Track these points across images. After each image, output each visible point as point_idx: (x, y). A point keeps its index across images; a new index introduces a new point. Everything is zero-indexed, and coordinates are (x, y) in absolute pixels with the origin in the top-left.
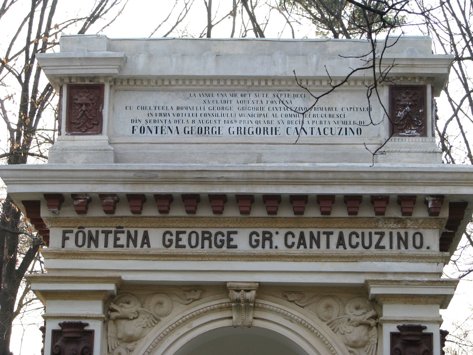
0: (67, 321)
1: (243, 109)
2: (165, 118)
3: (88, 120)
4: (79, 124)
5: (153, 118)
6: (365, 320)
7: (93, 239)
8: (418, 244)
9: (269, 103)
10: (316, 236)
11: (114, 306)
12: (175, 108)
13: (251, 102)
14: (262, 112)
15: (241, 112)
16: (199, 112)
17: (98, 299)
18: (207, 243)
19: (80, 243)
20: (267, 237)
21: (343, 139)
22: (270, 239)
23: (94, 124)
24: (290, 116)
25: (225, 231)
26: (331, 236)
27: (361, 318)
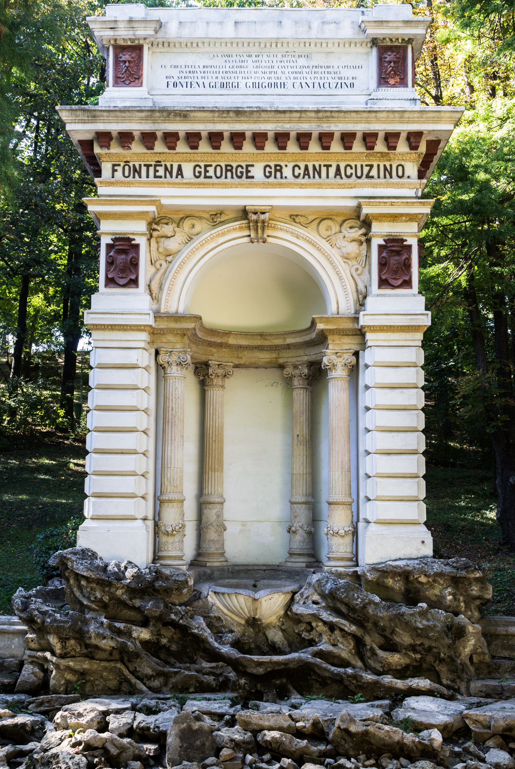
0: (118, 236)
1: (257, 67)
2: (194, 75)
3: (131, 75)
4: (123, 78)
5: (183, 75)
6: (357, 236)
8: (400, 174)
9: (278, 62)
11: (155, 226)
12: (201, 67)
13: (263, 62)
14: (272, 70)
15: (256, 70)
18: (229, 174)
19: (127, 174)
20: (279, 169)
21: (339, 91)
22: (280, 171)
23: (135, 78)
24: (296, 73)
25: (244, 165)
26: (330, 168)
27: (354, 235)
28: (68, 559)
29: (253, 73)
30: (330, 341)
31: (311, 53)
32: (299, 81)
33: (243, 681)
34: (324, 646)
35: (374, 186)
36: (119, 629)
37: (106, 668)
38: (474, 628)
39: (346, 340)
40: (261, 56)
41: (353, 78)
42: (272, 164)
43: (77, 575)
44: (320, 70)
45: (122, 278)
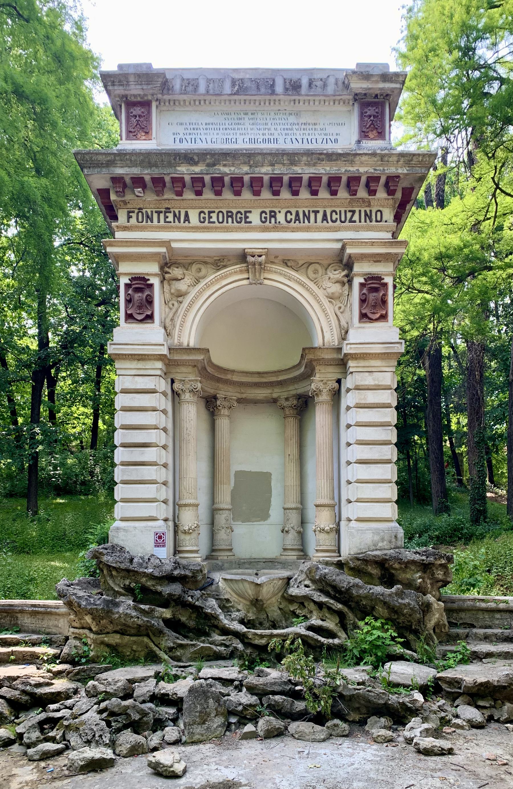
1: (253, 124)
2: (197, 131)
7: (150, 218)
8: (379, 218)
10: (307, 214)
12: (204, 124)
14: (267, 127)
16: (221, 127)
17: (155, 261)
18: (230, 220)
20: (273, 215)
22: (275, 217)
24: (287, 129)
25: (243, 211)
28: (101, 553)
29: (249, 129)
30: (317, 371)
31: (300, 111)
32: (290, 137)
33: (248, 651)
34: (315, 621)
35: (357, 230)
36: (144, 610)
37: (135, 642)
38: (438, 605)
39: (331, 369)
40: (256, 114)
41: (337, 134)
42: (267, 210)
43: (110, 566)
44: (308, 127)
45: (139, 314)
